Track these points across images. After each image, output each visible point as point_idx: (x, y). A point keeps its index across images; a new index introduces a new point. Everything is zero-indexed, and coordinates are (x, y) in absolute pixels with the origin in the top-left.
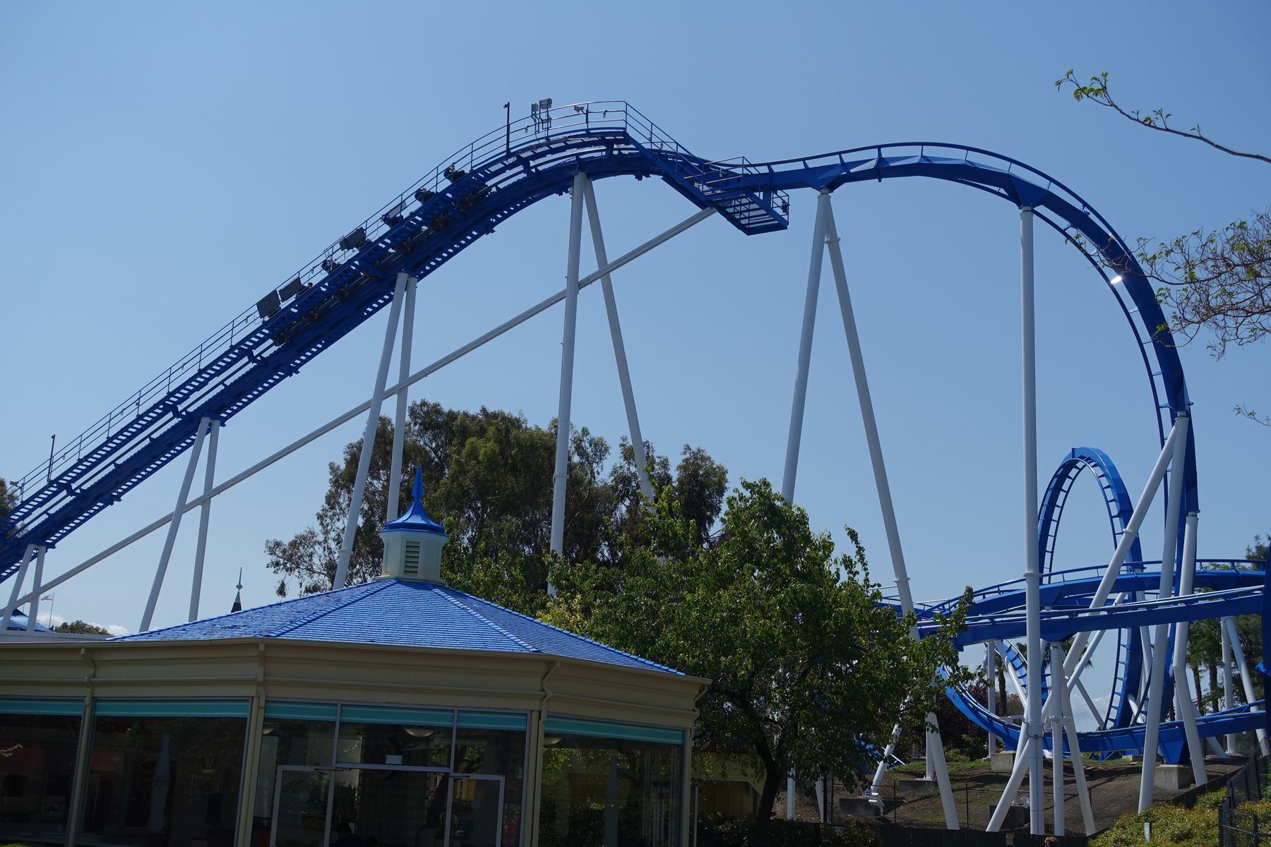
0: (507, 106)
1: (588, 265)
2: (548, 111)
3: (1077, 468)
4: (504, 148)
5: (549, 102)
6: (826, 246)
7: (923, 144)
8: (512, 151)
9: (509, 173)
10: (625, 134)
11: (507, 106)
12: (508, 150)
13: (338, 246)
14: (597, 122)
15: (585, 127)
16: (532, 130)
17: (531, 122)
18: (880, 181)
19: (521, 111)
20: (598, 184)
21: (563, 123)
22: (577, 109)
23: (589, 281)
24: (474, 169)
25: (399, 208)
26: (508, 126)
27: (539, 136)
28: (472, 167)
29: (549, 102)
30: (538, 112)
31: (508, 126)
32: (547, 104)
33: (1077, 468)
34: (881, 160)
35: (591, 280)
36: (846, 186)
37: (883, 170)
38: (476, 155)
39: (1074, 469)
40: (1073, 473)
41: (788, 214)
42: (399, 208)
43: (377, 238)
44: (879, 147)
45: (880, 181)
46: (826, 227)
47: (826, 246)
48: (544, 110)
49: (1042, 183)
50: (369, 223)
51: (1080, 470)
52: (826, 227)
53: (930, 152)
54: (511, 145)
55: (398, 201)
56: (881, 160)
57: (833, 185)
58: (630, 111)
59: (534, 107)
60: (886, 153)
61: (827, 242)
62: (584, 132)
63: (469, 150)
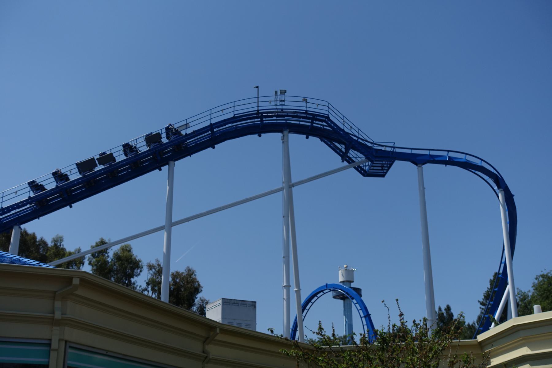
0: (257, 87)
8: (260, 111)
10: (328, 117)
11: (257, 87)
15: (305, 109)
16: (273, 103)
17: (273, 99)
18: (446, 166)
24: (236, 116)
25: (185, 127)
27: (278, 107)
28: (235, 115)
29: (285, 91)
32: (283, 92)
38: (236, 108)
45: (446, 166)
55: (184, 123)
59: (276, 92)
62: (304, 112)
63: (232, 105)
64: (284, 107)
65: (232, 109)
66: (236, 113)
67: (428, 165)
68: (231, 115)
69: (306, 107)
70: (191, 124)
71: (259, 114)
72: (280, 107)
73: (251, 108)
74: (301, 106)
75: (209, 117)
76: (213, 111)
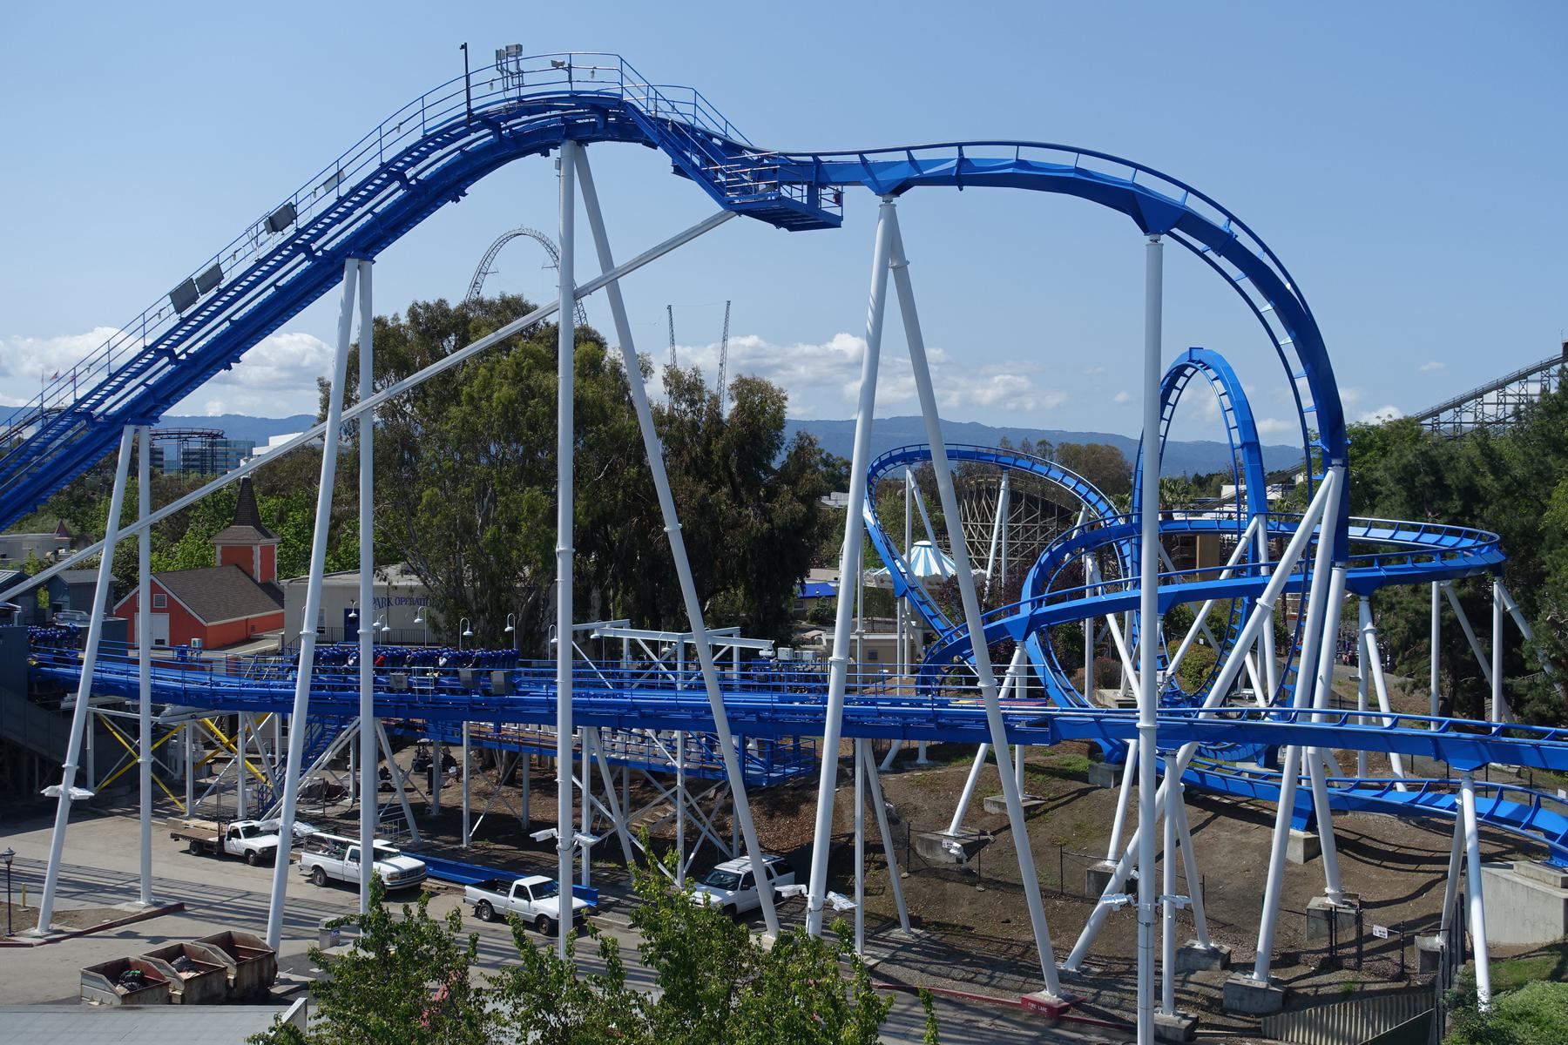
0: (464, 47)
1: (587, 269)
2: (518, 61)
3: (1185, 376)
4: (464, 109)
5: (519, 48)
6: (891, 271)
7: (1018, 144)
8: (476, 112)
9: (474, 136)
11: (464, 47)
12: (470, 111)
13: (262, 226)
14: (585, 84)
15: (567, 87)
16: (498, 86)
18: (961, 190)
19: (483, 57)
20: (595, 150)
21: (541, 80)
22: (556, 65)
23: (588, 290)
24: (428, 133)
25: (335, 181)
26: (467, 76)
27: (510, 94)
28: (425, 131)
29: (519, 48)
30: (504, 61)
31: (467, 76)
33: (1185, 376)
34: (962, 161)
35: (590, 289)
36: (915, 189)
37: (965, 175)
38: (429, 113)
39: (1182, 378)
40: (1181, 382)
41: (841, 206)
42: (335, 181)
43: (311, 218)
44: (960, 145)
45: (961, 190)
46: (893, 245)
47: (891, 271)
48: (513, 59)
49: (1174, 194)
50: (301, 196)
51: (1189, 378)
52: (893, 245)
53: (1027, 154)
54: (474, 105)
55: (334, 170)
56: (962, 161)
57: (900, 188)
58: (626, 69)
60: (969, 153)
61: (893, 268)
63: (418, 106)
64: (524, 91)
65: (419, 119)
66: (428, 125)
67: (916, 190)
68: (417, 136)
69: (570, 82)
70: (346, 172)
71: (474, 120)
72: (513, 93)
73: (449, 109)
74: (556, 83)
75: (377, 148)
76: (385, 129)
